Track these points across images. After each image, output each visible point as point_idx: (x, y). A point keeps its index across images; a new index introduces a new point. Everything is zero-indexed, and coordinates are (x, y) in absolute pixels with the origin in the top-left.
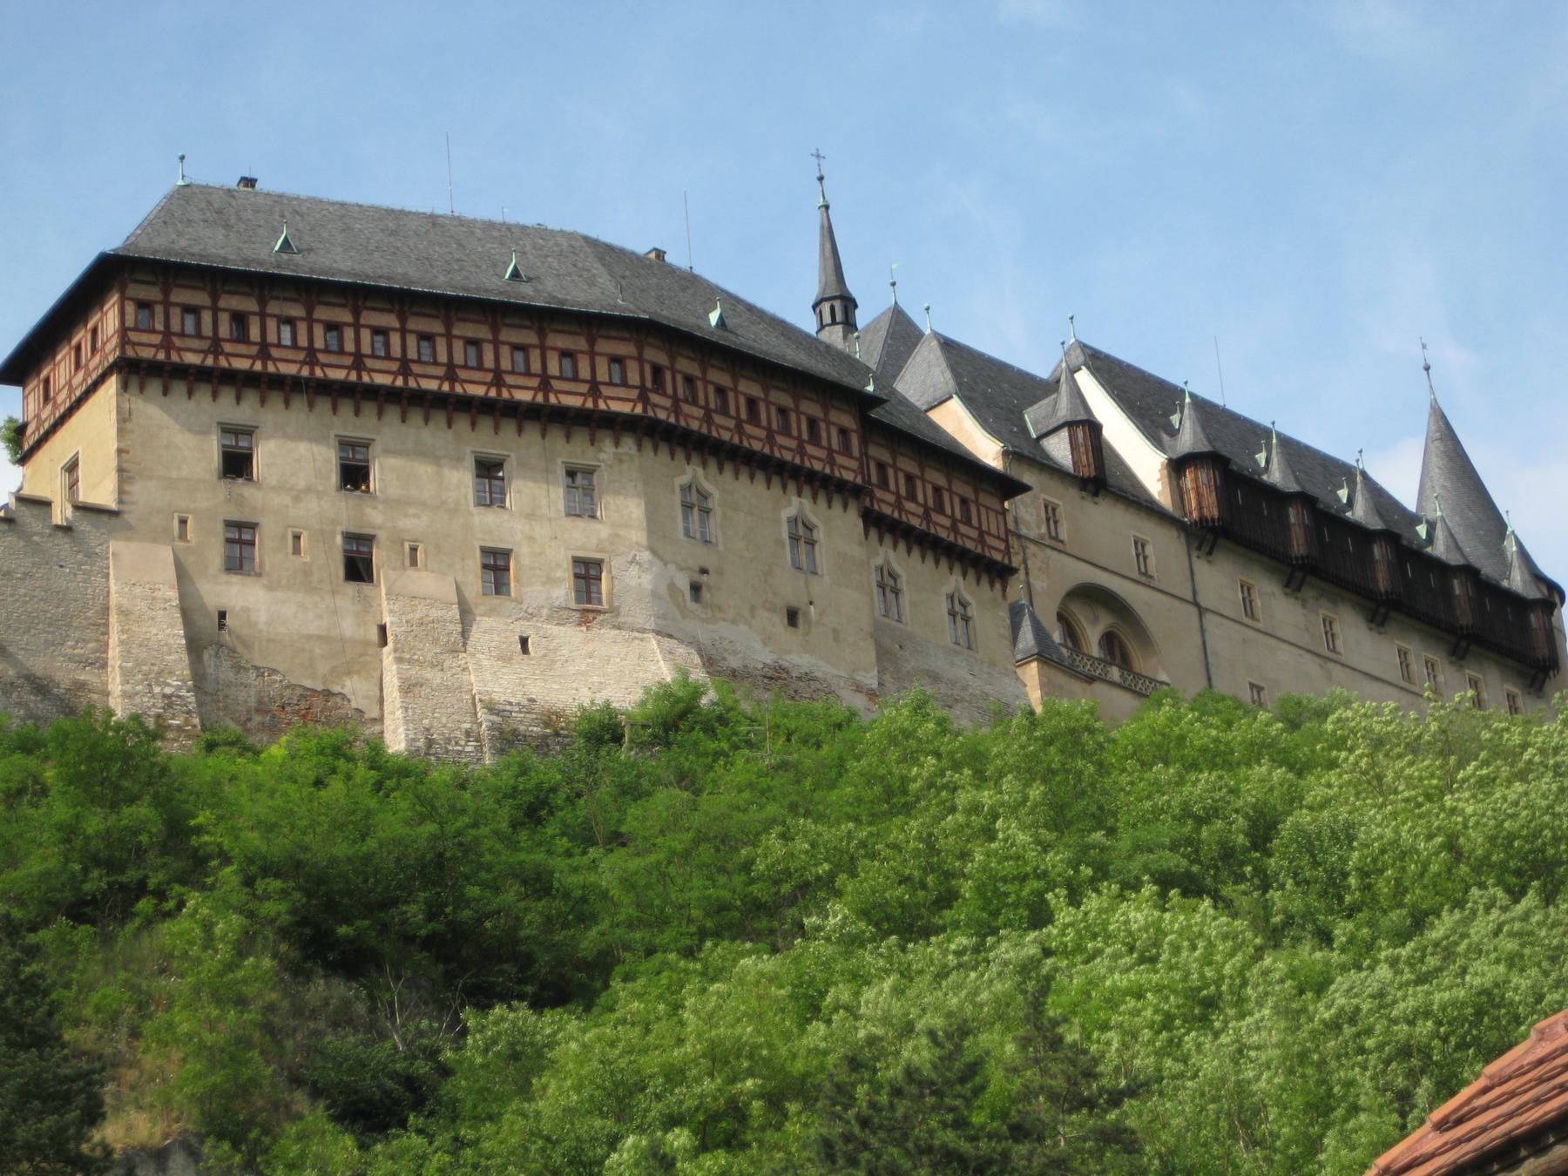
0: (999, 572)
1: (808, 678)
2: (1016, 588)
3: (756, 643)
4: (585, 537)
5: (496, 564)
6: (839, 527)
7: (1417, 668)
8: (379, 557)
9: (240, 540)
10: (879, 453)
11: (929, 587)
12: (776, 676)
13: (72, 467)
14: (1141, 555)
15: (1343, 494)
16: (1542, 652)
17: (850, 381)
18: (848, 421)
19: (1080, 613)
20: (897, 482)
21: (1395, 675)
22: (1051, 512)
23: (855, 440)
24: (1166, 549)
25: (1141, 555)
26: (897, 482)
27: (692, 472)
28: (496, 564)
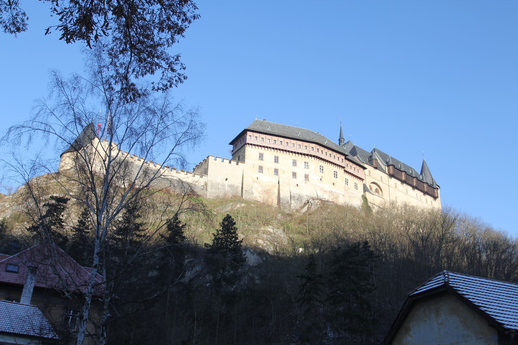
0: (362, 179)
1: (335, 192)
2: (364, 181)
3: (328, 187)
4: (306, 171)
5: (294, 174)
6: (340, 171)
7: (419, 196)
8: (279, 172)
9: (261, 168)
10: (347, 162)
11: (352, 180)
12: (331, 192)
13: (239, 157)
14: (382, 178)
15: (410, 172)
16: (436, 195)
17: (343, 152)
18: (343, 157)
19: (372, 185)
20: (349, 166)
21: (415, 197)
22: (370, 172)
23: (344, 160)
24: (385, 177)
25: (382, 178)
26: (349, 166)
27: (322, 163)
28: (294, 174)
